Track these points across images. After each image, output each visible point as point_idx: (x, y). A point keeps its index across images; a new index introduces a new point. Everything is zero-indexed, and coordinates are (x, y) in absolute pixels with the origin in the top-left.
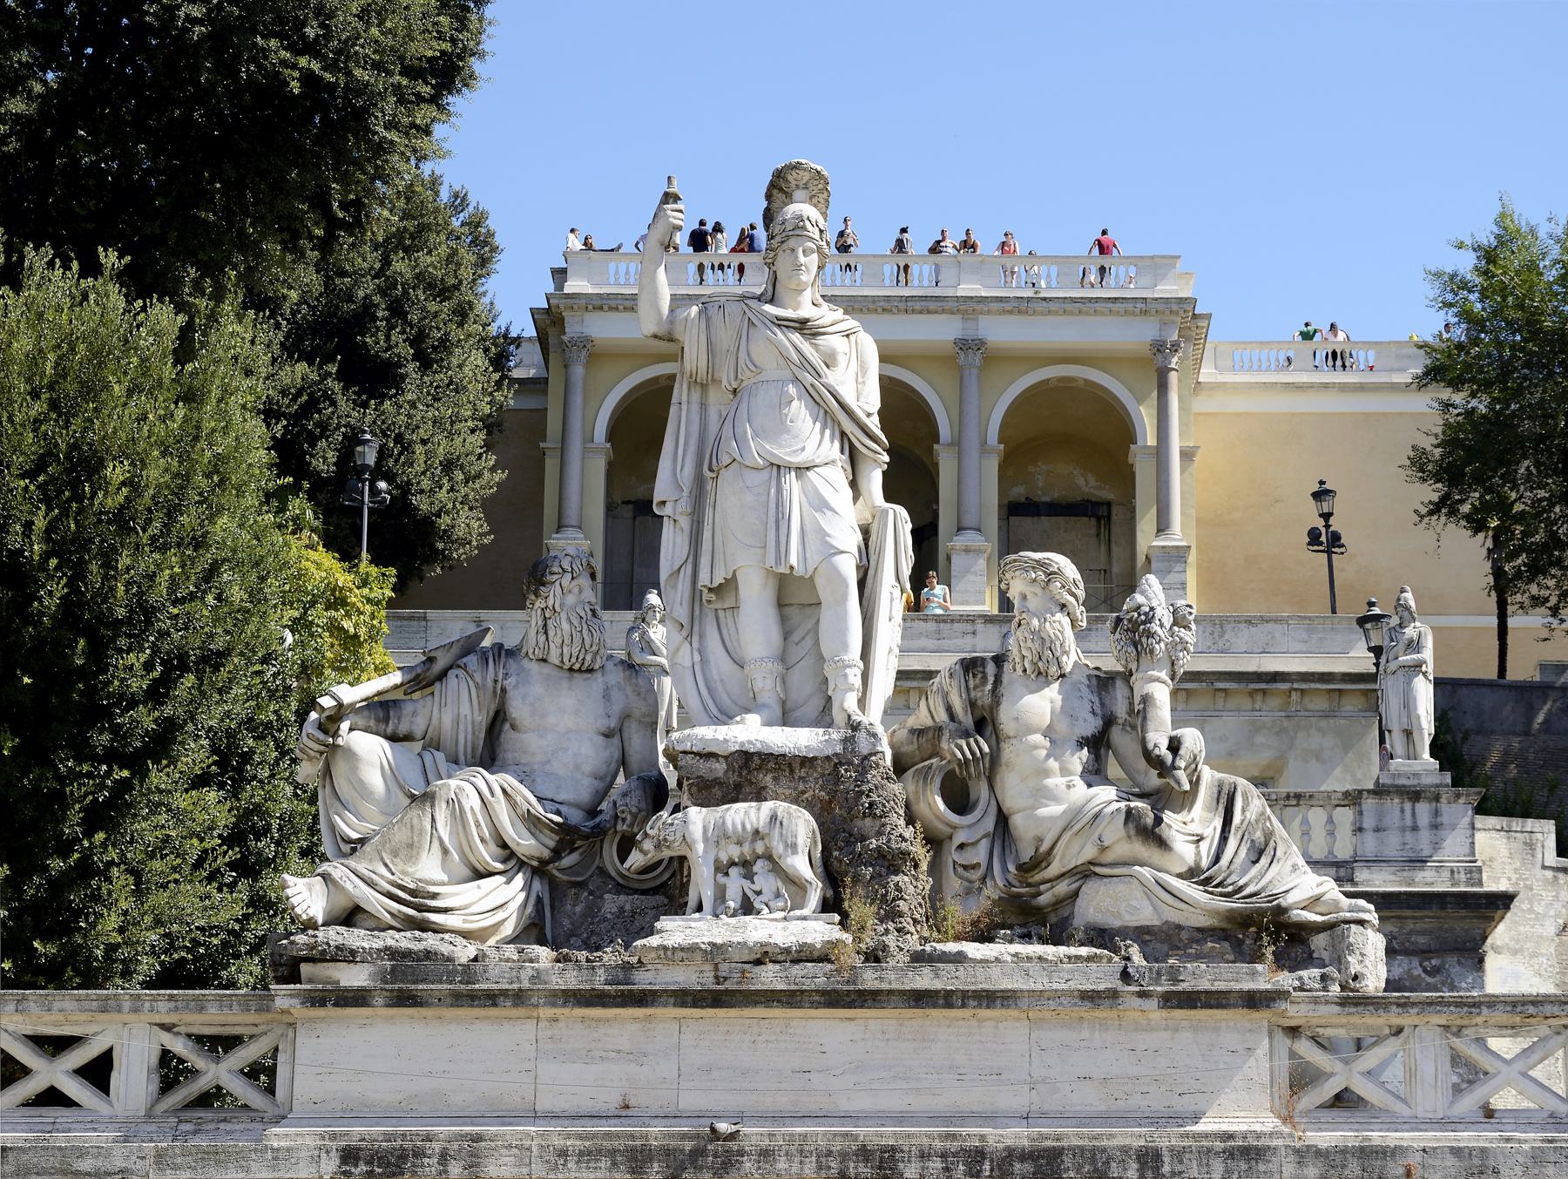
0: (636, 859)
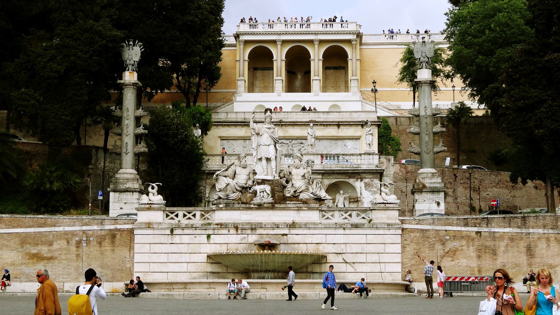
0: (251, 191)
